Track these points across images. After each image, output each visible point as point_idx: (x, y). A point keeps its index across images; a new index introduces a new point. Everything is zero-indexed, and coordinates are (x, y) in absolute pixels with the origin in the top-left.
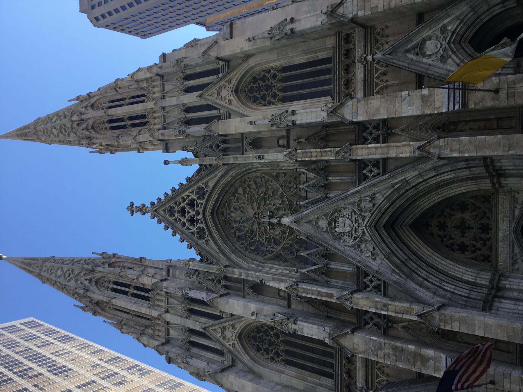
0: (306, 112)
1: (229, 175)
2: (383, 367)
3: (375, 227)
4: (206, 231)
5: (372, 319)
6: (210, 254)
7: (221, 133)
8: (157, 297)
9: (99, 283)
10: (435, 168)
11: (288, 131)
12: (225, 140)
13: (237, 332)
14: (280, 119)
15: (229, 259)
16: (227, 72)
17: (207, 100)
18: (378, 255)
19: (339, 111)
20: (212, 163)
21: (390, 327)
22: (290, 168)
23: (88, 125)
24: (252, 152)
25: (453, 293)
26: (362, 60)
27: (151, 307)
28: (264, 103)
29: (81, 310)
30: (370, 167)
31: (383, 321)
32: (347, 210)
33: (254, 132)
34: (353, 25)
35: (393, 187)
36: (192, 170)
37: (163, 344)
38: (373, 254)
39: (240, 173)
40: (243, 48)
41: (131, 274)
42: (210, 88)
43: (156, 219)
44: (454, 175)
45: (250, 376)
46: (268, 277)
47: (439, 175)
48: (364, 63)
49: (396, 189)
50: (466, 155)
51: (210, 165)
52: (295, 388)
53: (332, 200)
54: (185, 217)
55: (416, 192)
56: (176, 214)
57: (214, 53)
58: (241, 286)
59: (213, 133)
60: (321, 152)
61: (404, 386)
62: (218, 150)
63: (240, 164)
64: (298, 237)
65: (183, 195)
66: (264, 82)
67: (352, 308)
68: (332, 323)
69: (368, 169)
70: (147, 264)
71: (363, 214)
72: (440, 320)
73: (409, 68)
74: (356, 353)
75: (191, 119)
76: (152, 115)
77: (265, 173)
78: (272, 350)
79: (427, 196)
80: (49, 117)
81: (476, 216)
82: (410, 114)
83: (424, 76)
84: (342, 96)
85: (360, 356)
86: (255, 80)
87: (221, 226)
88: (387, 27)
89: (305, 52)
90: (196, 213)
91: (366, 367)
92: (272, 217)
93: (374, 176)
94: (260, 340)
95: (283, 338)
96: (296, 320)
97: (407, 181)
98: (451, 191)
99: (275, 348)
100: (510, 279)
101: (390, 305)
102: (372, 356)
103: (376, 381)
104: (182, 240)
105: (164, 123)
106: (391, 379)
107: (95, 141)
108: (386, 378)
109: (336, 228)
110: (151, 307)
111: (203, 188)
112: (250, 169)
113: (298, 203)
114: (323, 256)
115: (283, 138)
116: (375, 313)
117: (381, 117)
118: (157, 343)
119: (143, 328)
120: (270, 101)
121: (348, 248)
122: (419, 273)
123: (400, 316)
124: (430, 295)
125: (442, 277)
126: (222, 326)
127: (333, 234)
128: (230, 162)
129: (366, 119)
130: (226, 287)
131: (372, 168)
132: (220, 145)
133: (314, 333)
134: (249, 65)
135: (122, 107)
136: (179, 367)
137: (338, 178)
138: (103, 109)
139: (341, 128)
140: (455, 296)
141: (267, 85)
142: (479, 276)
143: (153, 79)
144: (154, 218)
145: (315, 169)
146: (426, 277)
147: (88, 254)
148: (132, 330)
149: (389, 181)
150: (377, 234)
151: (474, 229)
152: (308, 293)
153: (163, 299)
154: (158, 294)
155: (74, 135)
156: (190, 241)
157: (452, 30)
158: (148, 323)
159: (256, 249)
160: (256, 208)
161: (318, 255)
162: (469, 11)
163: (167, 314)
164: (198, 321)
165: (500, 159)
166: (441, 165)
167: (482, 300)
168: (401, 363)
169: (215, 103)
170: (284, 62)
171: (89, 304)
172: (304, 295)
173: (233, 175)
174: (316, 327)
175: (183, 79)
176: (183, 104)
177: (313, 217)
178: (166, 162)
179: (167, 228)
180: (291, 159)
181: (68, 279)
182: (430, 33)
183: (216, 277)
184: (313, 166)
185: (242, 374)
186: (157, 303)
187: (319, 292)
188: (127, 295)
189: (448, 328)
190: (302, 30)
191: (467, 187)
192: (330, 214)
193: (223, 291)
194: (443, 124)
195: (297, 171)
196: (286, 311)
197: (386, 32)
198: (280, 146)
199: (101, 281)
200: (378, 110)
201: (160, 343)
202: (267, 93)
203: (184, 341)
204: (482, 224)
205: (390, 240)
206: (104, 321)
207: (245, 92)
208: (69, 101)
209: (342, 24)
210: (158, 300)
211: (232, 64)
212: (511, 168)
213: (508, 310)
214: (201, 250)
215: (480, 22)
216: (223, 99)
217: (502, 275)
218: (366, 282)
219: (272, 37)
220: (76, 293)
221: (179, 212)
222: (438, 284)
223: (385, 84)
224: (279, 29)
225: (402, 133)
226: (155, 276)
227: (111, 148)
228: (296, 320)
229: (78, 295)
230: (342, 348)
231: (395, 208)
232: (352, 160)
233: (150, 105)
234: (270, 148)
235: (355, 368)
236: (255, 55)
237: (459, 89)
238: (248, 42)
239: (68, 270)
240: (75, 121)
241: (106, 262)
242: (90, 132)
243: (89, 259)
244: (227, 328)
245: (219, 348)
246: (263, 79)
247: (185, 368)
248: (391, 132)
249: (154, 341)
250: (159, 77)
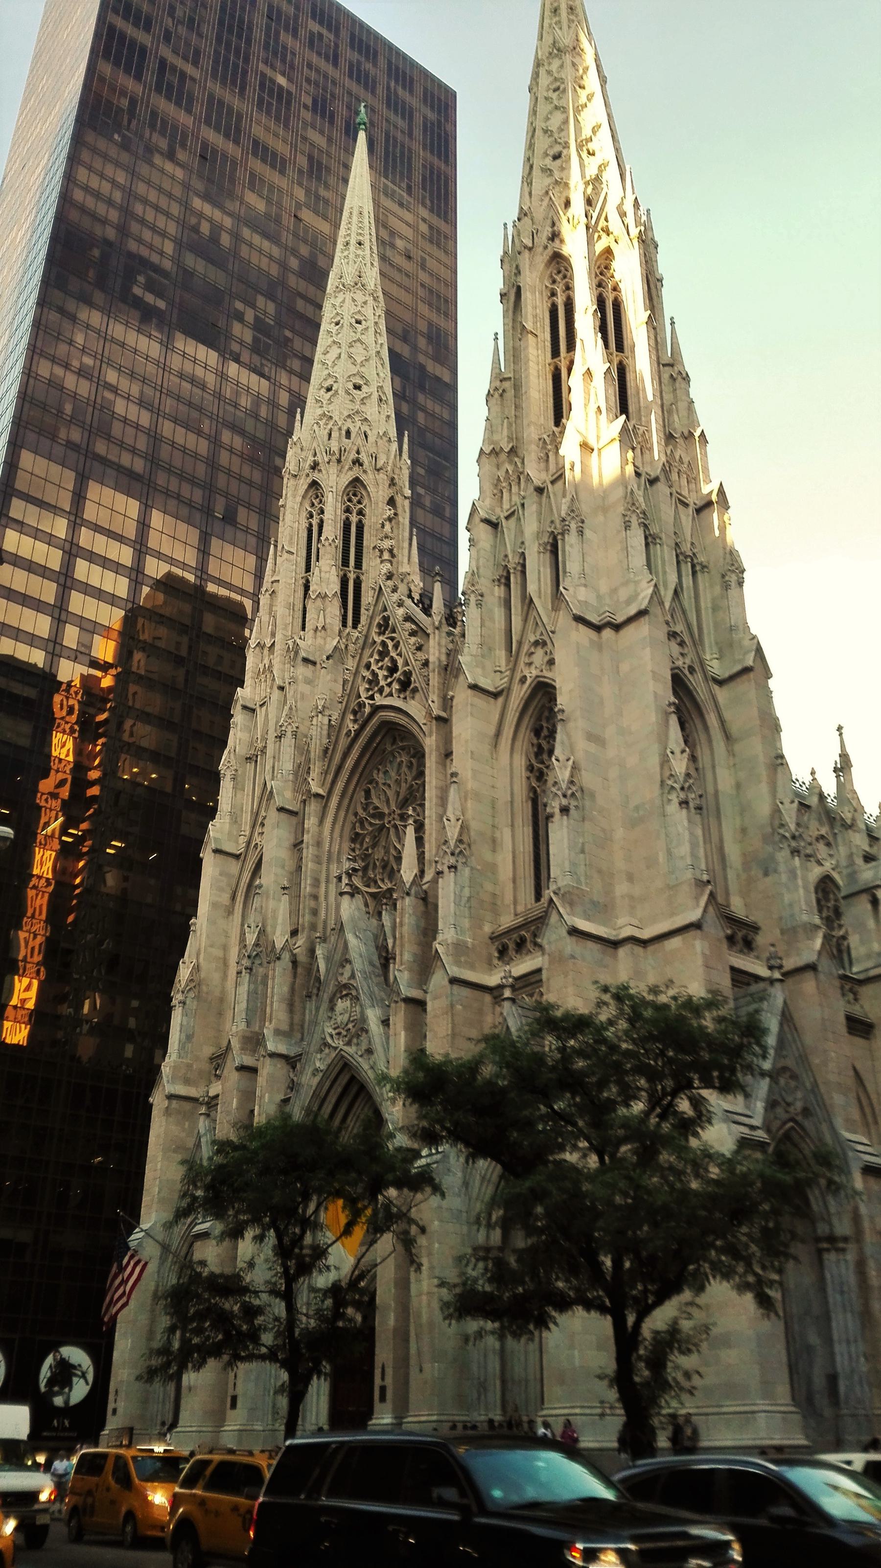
15: (330, 792)
38: (317, 1070)
56: (382, 638)
71: (355, 1040)
87: (376, 748)
109: (341, 998)
127: (334, 995)
159: (357, 834)
205: (340, 1090)
226: (318, 633)
241: (361, 465)
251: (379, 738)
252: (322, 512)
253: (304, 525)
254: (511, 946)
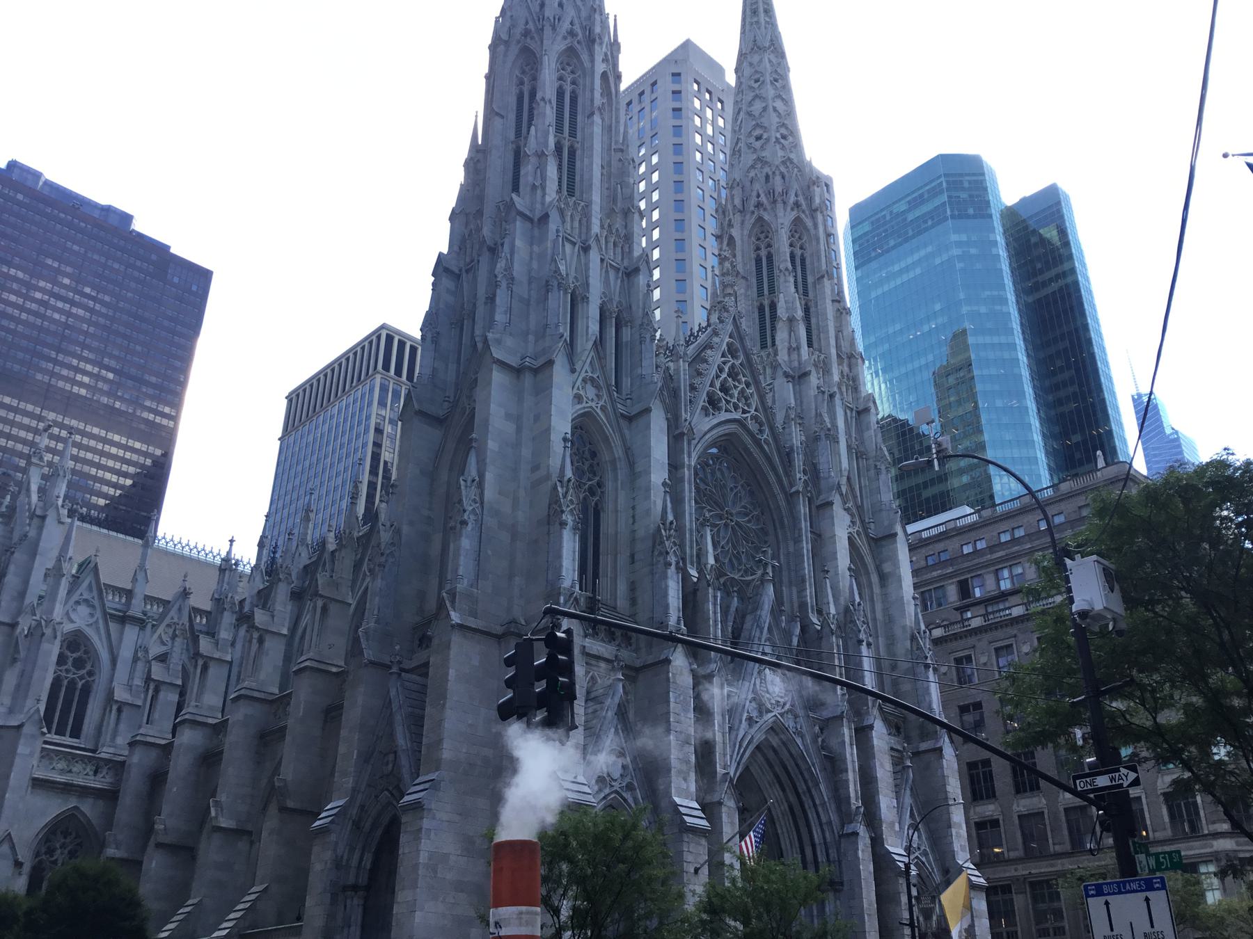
10: (830, 823)
23: (803, 212)
47: (821, 824)
50: (861, 867)
55: (800, 791)
72: (729, 807)
111: (761, 431)
126: (601, 383)
176: (838, 438)
221: (733, 366)
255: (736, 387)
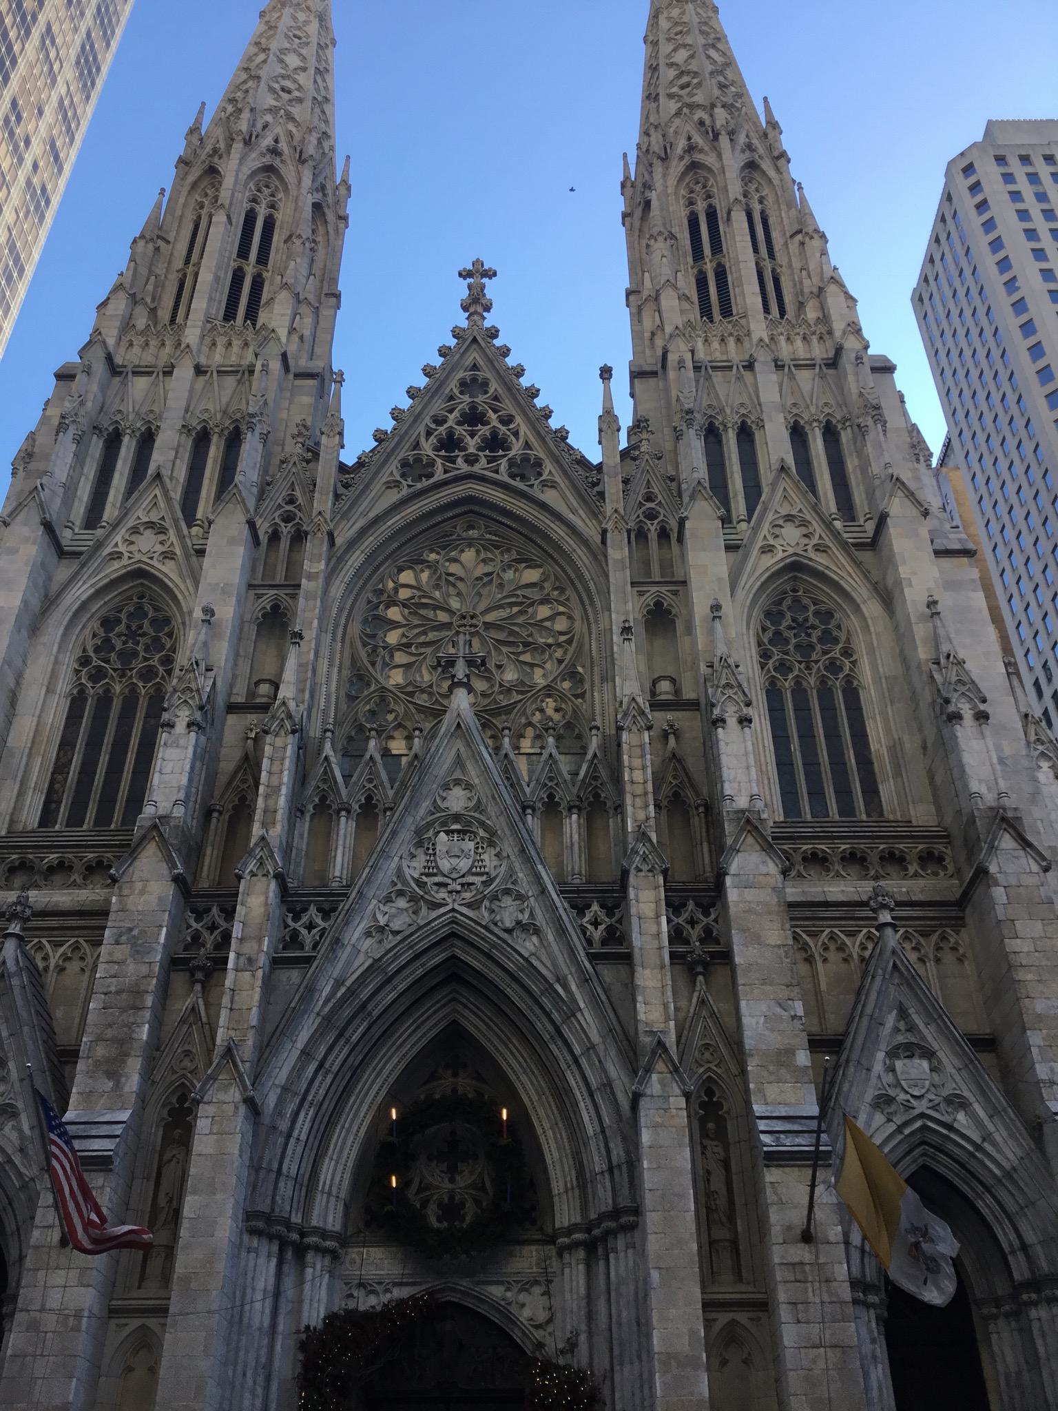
0: (746, 754)
1: (575, 546)
2: (82, 959)
3: (453, 935)
4: (425, 483)
5: (212, 928)
6: (362, 492)
7: (688, 524)
8: (237, 343)
9: (269, 177)
10: (608, 1085)
11: (694, 705)
12: (668, 537)
13: (153, 566)
14: (728, 685)
15: (352, 544)
16: (846, 543)
17: (774, 485)
18: (380, 942)
19: (750, 840)
20: (607, 500)
21: (193, 975)
22: (598, 711)
23: (701, 151)
24: (637, 609)
25: (289, 1136)
26: (880, 899)
27: (209, 326)
28: (766, 641)
29: (190, 122)
30: (607, 919)
31: (207, 958)
32: (495, 863)
33: (691, 614)
34: (969, 875)
35: (558, 980)
36: (588, 444)
37: (109, 358)
38: (381, 930)
39: (580, 577)
40: (910, 585)
41: (297, 268)
42: (804, 494)
43: (452, 342)
44: (590, 1132)
45: (35, 603)
46: (308, 652)
47: (591, 1095)
48: (872, 903)
49: (551, 986)
50: (645, 1164)
51: (601, 495)
52: (11, 723)
53: (520, 825)
54: (459, 423)
55: (547, 1037)
56: (467, 398)
57: (897, 507)
58: (280, 578)
59: (688, 504)
60: (646, 794)
61: (37, 1012)
62: (642, 518)
63: (607, 576)
64: (417, 733)
65: (518, 419)
66: (820, 640)
67: (239, 878)
68: (194, 824)
69: (602, 915)
70: (324, 312)
71: (486, 903)
73: (861, 1016)
74: (120, 888)
75: (720, 442)
76: (731, 334)
77: (580, 646)
78: (107, 661)
79: (533, 1066)
80: (719, 39)
81: (483, 1189)
82: (746, 1020)
83: (838, 1053)
84: (785, 847)
85: (114, 899)
86: (829, 615)
88: (960, 960)
89: (895, 748)
90: (472, 454)
91: (81, 914)
92: (470, 663)
93: (584, 930)
94: (134, 628)
95: (143, 692)
96: (200, 728)
97: (574, 1015)
98: (547, 1126)
99: (115, 670)
100: (326, 1278)
101: (253, 976)
102: (115, 930)
103: (44, 941)
104: (396, 414)
105: (712, 367)
106: (51, 978)
107: (658, 169)
108: (52, 967)
109: (447, 833)
110: (209, 326)
111: (540, 474)
112: (592, 603)
113: (507, 732)
114: (369, 798)
115: (676, 692)
116: (227, 937)
117: (736, 949)
118: (111, 342)
119: (149, 300)
120: (770, 657)
121: (393, 866)
122: (336, 1051)
123: (226, 1000)
124: (282, 1076)
125: (328, 1106)
126: (168, 523)
127: (429, 825)
128: (609, 550)
129: (733, 910)
130: (275, 537)
131: (603, 926)
132: (656, 522)
133: (166, 778)
134: (865, 602)
135: (751, 250)
136: (47, 403)
137: (576, 837)
138: (745, 196)
139: (705, 845)
140: (281, 1140)
141: (811, 647)
142: (333, 1199)
143: (826, 337)
144: (454, 336)
145: (595, 778)
146: (327, 1065)
147: (343, 143)
148: (143, 271)
149: (573, 970)
150: (433, 938)
151: (450, 1186)
152: (271, 759)
153: (234, 359)
154: (246, 344)
155: (673, 112)
156: (396, 439)
157: (956, 1125)
158: (164, 314)
160: (490, 618)
161: (371, 786)
162: (1005, 1163)
163: (192, 370)
164: (176, 457)
165: (634, 1248)
166: (615, 1099)
167: (273, 1210)
168: (102, 1005)
169: (765, 509)
170: (871, 697)
171: (209, 148)
172: (268, 750)
173: (574, 557)
174: (185, 781)
175: (828, 422)
177: (473, 773)
178: (606, 373)
179: (428, 371)
180: (626, 714)
181: (276, 86)
182: (950, 1069)
183: (299, 508)
184: (604, 773)
185: (41, 582)
186: (221, 341)
187: (279, 788)
188: (239, 256)
189: (202, 1125)
190: (957, 744)
191: (558, 1167)
192: (483, 818)
193: (264, 528)
194: (719, 1105)
195: (591, 729)
196: (220, 701)
197: (948, 958)
198: (654, 683)
199: (275, 182)
200: (756, 939)
201: (111, 349)
202: (791, 647)
203: (118, 417)
204: (462, 1205)
205: (420, 972)
206: (163, 190)
207: (795, 591)
208: (765, 99)
209: (971, 847)
210: (230, 344)
211: (866, 556)
212: (613, 1274)
213: (250, 1275)
214: (373, 469)
215: (975, 1191)
216: (777, 531)
217: (334, 1256)
218: (309, 913)
219: (938, 663)
220: (240, 111)
221: (473, 406)
222: (310, 1097)
223: (817, 956)
224: (959, 681)
225: (694, 1000)
227: (638, 212)
228: (200, 728)
229: (231, 114)
230: (129, 850)
231: (502, 986)
232: (625, 874)
233: (759, 328)
234: (650, 657)
235: (74, 885)
236: (891, 618)
237: (817, 1145)
238: (925, 600)
239: (300, 88)
240: (711, 116)
241: (325, 195)
242: (682, 158)
243: (332, 148)
244: (162, 537)
245: (105, 517)
246: (828, 638)
247: (44, 420)
248: (700, 973)
249: (115, 332)
250: (831, 354)
251: (450, 514)
252: (272, 206)
253: (246, 206)
254: (798, 858)
255: (472, 436)
